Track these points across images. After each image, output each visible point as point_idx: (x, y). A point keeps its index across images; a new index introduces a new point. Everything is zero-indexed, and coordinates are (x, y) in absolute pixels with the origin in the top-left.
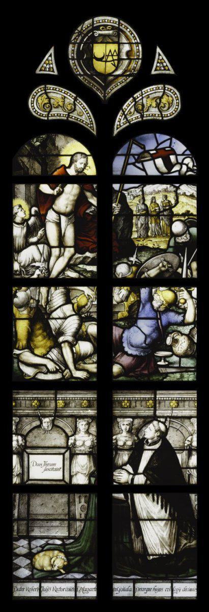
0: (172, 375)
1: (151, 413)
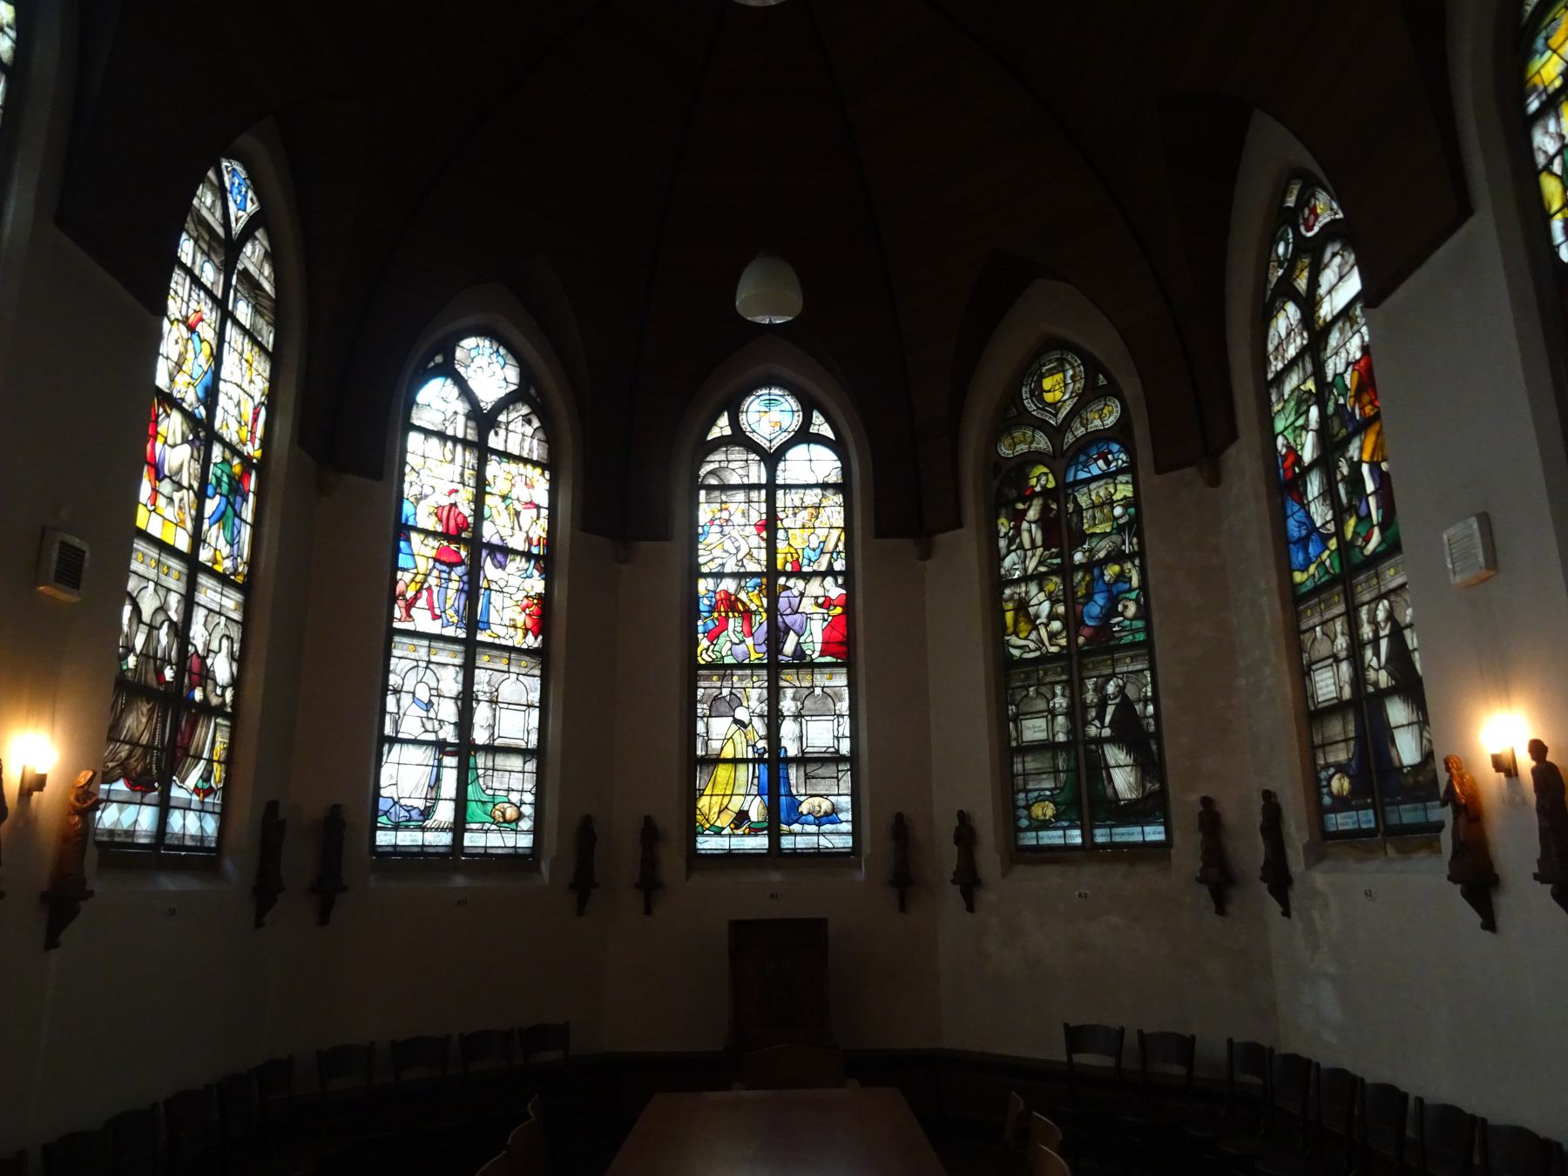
1: (1109, 671)
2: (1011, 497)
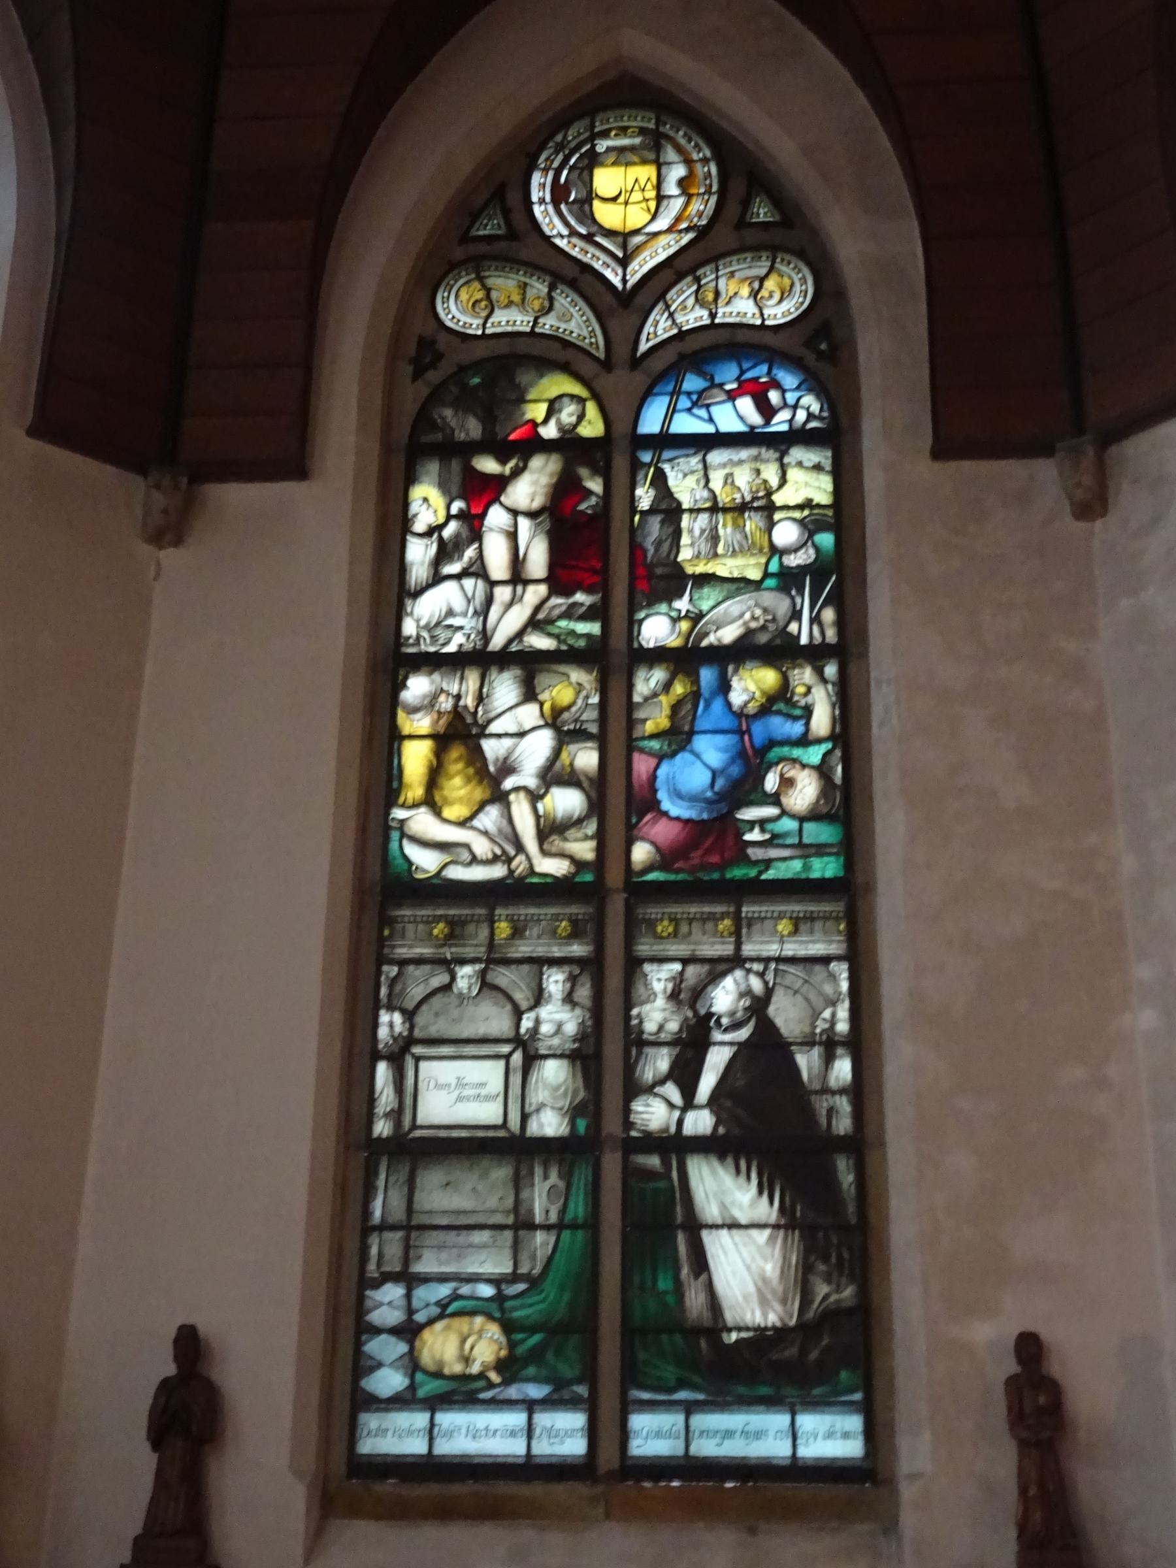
0: (782, 865)
1: (727, 949)
2: (461, 436)
